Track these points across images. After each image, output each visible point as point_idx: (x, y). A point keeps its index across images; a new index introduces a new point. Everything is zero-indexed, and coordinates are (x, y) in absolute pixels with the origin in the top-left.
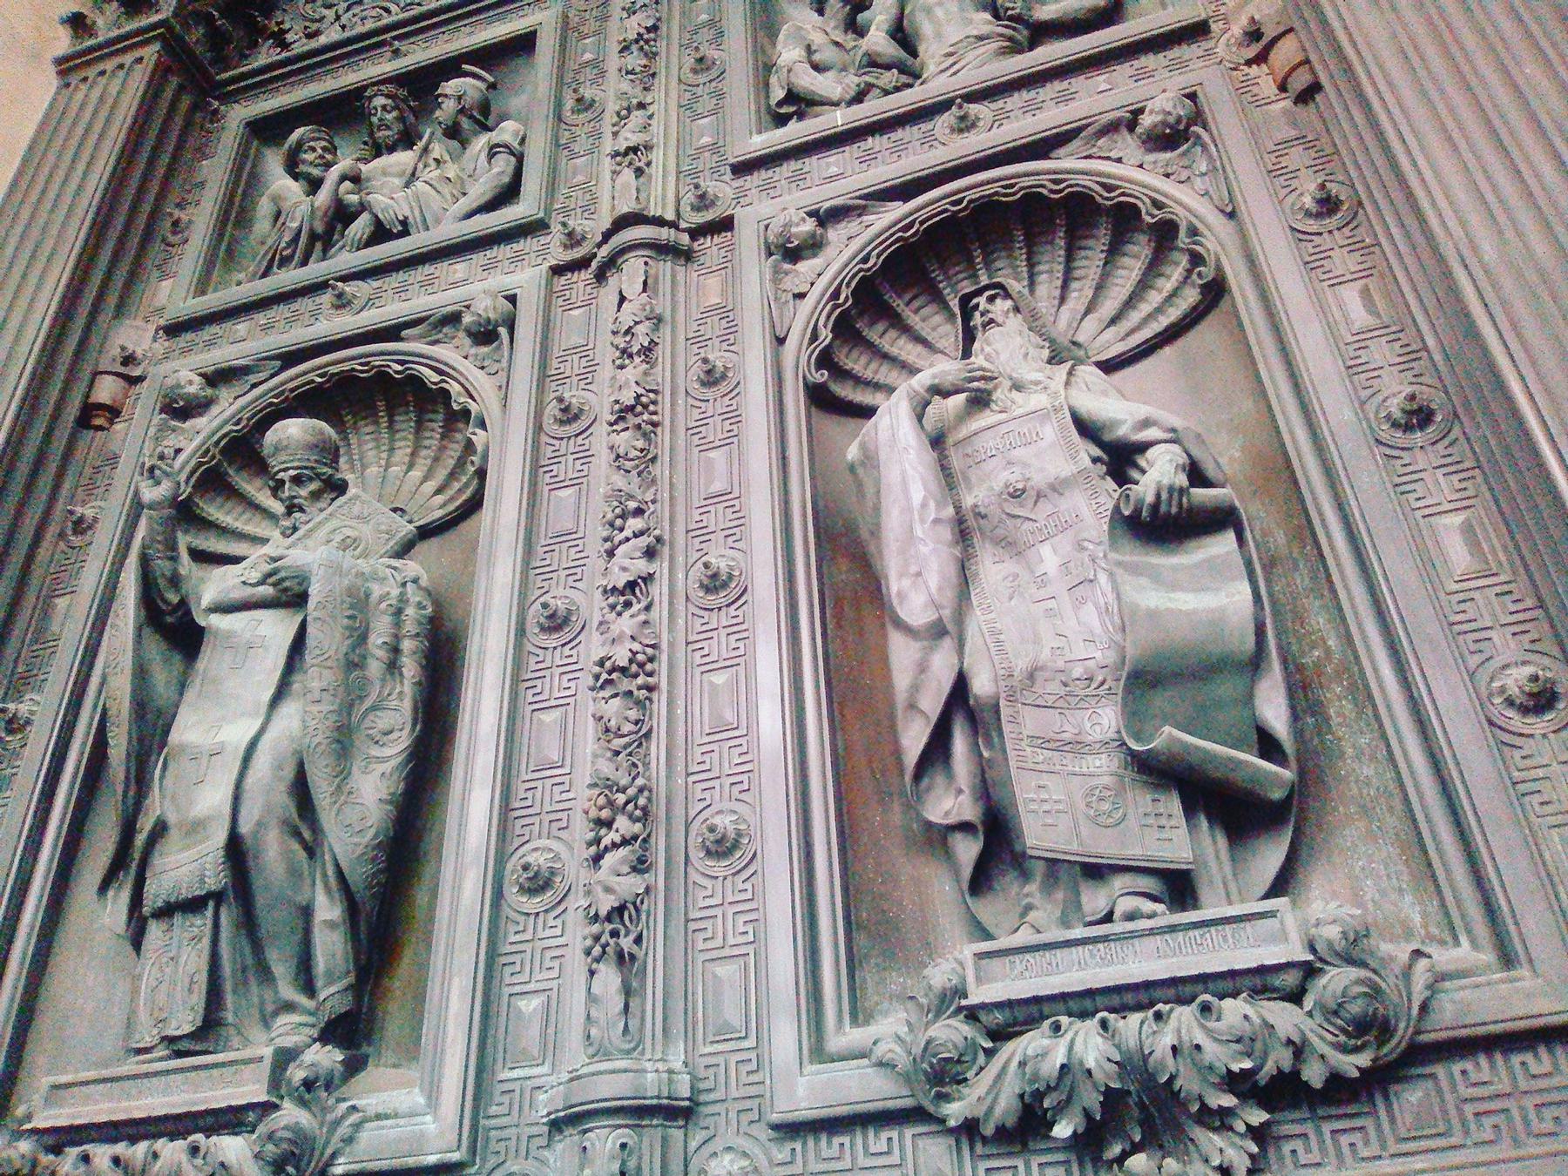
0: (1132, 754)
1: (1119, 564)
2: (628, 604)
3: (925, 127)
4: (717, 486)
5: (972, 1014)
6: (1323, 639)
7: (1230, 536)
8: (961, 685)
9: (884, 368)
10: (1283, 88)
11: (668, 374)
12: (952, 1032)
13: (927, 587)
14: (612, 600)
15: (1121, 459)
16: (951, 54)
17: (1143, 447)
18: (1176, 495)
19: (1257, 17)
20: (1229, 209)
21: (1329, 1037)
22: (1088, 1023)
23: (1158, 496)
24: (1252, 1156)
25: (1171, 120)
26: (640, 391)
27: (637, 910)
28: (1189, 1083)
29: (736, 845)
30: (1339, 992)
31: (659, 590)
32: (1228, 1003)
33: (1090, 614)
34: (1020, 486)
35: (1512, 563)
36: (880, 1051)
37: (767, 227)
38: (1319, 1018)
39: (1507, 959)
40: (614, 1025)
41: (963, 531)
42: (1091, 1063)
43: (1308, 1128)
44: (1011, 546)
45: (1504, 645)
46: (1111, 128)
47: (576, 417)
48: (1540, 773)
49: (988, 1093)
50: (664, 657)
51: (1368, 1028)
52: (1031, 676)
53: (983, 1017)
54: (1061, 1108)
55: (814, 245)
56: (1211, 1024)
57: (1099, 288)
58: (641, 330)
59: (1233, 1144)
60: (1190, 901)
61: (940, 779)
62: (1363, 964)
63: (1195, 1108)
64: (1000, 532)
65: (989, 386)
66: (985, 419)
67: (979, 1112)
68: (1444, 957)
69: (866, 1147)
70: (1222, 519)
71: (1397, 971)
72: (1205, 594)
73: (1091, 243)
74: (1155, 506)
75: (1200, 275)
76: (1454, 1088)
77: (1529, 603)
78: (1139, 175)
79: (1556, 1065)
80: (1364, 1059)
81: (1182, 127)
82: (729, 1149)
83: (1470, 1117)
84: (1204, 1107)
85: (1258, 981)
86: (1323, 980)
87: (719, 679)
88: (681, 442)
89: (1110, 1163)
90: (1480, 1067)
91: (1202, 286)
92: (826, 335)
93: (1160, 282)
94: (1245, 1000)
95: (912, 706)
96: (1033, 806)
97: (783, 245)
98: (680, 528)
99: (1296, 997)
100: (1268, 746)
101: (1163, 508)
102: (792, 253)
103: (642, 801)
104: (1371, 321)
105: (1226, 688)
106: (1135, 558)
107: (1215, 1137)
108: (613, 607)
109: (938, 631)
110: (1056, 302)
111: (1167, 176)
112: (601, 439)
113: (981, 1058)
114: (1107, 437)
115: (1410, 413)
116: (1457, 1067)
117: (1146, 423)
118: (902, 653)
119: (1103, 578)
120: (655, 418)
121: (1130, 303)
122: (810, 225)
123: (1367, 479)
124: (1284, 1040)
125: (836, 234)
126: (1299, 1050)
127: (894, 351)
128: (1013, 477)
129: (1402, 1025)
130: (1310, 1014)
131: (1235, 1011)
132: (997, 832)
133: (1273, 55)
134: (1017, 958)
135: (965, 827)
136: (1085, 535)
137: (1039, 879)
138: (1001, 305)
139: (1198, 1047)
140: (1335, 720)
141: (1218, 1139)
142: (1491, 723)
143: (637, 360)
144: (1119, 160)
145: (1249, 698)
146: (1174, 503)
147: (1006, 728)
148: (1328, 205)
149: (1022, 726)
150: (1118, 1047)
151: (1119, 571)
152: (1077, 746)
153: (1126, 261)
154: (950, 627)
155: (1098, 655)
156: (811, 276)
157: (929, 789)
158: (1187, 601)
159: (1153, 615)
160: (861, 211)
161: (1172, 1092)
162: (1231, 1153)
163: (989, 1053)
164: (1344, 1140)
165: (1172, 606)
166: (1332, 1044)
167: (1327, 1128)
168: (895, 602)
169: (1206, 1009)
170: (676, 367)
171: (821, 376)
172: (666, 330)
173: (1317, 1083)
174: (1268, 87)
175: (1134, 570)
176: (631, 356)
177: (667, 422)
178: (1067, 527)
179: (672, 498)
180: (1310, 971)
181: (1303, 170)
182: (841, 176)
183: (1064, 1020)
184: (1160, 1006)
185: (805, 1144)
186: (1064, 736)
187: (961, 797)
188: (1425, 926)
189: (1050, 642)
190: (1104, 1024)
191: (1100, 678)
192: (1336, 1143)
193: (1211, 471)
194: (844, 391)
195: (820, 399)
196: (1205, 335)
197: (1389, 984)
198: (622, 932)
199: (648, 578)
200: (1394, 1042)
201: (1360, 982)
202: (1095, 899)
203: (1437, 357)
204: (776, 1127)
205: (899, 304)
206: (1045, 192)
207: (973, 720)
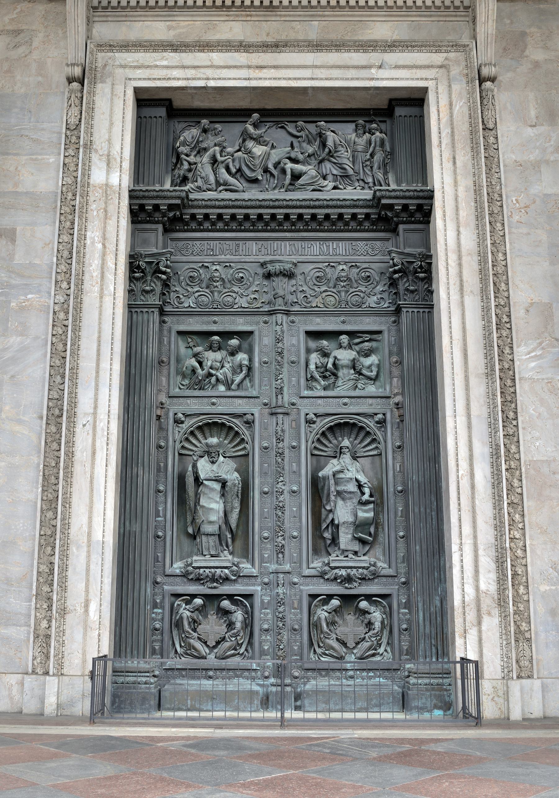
8: (333, 520)
12: (327, 568)
28: (354, 578)
31: (285, 492)
37: (307, 414)
39: (390, 567)
51: (374, 574)
55: (314, 422)
90: (384, 578)
95: (324, 520)
109: (331, 511)
117: (365, 483)
118: (324, 512)
123: (392, 501)
125: (318, 420)
131: (360, 570)
132: (335, 541)
148: (399, 447)
175: (360, 509)
202: (346, 554)
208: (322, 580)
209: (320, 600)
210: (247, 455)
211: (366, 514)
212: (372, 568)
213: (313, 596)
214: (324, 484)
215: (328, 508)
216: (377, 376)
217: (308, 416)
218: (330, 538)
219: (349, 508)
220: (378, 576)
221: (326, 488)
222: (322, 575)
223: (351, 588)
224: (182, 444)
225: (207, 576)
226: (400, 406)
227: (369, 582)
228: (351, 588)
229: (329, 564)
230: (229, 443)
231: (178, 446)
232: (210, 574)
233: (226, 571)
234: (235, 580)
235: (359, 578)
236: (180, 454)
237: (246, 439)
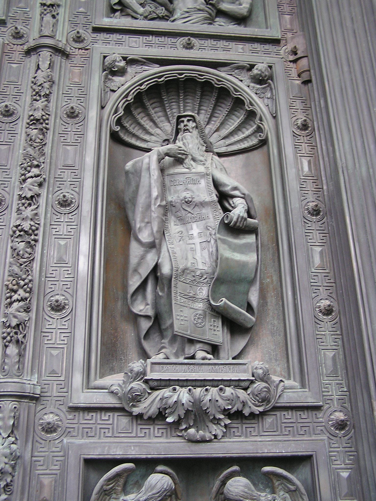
0: (210, 304)
1: (219, 239)
2: (30, 205)
3: (173, 40)
4: (70, 162)
5: (146, 382)
6: (271, 276)
7: (254, 237)
8: (156, 268)
9: (140, 131)
10: (299, 76)
11: (54, 107)
13: (152, 229)
14: (23, 201)
15: (224, 198)
16: (188, 12)
17: (233, 197)
18: (243, 220)
19: (297, 47)
20: (274, 115)
21: (253, 402)
22: (184, 389)
23: (238, 219)
24: (223, 432)
25: (263, 75)
26: (44, 113)
27: (25, 326)
28: (212, 411)
29: (64, 308)
30: (260, 388)
31: (42, 201)
32: (227, 389)
33: (206, 253)
34: (190, 199)
35: (330, 266)
36: (113, 388)
37: (105, 57)
38: (251, 396)
39: (303, 386)
40: (14, 366)
41: (167, 209)
42: (184, 402)
43: (239, 425)
44: (182, 221)
45: (323, 292)
46: (240, 68)
47: (11, 115)
48: (323, 333)
49: (148, 406)
50: (41, 229)
51: (266, 400)
52: (183, 271)
53: (151, 383)
54: (171, 414)
55: (122, 72)
56: (221, 394)
57: (222, 124)
58: (46, 85)
59: (219, 429)
60: (216, 354)
61: (140, 298)
62: (266, 382)
63: (212, 417)
64: (179, 214)
65: (184, 157)
66: (180, 169)
67: (144, 412)
68: (287, 383)
69: (101, 417)
70: (253, 230)
71: (275, 384)
72: (243, 254)
73: (223, 105)
74: (236, 222)
75: (260, 135)
76: (281, 419)
77: (332, 281)
78: (246, 89)
79: (308, 416)
80: (261, 409)
81: (266, 79)
82: (52, 413)
83: (283, 427)
84: (214, 418)
85: (237, 383)
86: (255, 385)
87: (62, 242)
88: (56, 139)
89: (182, 430)
90: (289, 414)
91: (259, 140)
92: (121, 112)
93: (244, 130)
94: (232, 389)
95: (136, 270)
96: (178, 318)
97: (111, 68)
98: (52, 176)
99: (246, 389)
100: (249, 308)
101: (238, 224)
102: (112, 71)
103: (30, 285)
104: (309, 174)
105: (242, 288)
106: (224, 238)
107: (214, 426)
108: (23, 204)
109: (152, 246)
110: (206, 123)
111: (256, 94)
112: (21, 127)
113: (147, 395)
114: (221, 189)
115: (315, 210)
116: (283, 413)
117: (235, 189)
118: (135, 250)
119: (213, 242)
120: (47, 126)
121: (231, 134)
122: (122, 64)
123: (298, 229)
124: (242, 402)
125: (131, 70)
126: (244, 404)
127: (142, 122)
128: (187, 195)
129: (273, 401)
130: (249, 394)
131: (229, 391)
133: (299, 62)
134: (165, 366)
135: (147, 317)
136: (209, 224)
137: (168, 339)
138: (191, 124)
139: (217, 401)
140: (269, 304)
141: (215, 427)
142: (315, 316)
143: (43, 99)
144: (241, 81)
145: (247, 293)
146: (242, 223)
147: (173, 288)
148: (305, 127)
149: (178, 288)
150: (193, 397)
151: (219, 241)
152: (193, 298)
153: (234, 117)
154: (158, 246)
155: (206, 268)
156: (118, 84)
157: (135, 300)
158: (238, 257)
159: (227, 259)
160: (143, 64)
161: (206, 412)
162: (218, 430)
163: (149, 394)
164: (249, 430)
165: (233, 257)
166: (253, 404)
167: (244, 426)
168: (137, 231)
169: (221, 389)
170: (58, 105)
171: (118, 128)
172: (55, 88)
173: (247, 414)
174: (294, 73)
175: (224, 242)
176: (40, 96)
177: (52, 129)
178: (203, 219)
179: (51, 163)
180: (252, 382)
181: (299, 110)
182: (137, 47)
183: (177, 387)
184: (207, 387)
185: (79, 414)
186: (191, 294)
187: (148, 307)
188: (281, 371)
189: (191, 260)
190: (190, 390)
191: (205, 277)
192: (246, 430)
193: (252, 213)
194: (122, 135)
195: (115, 137)
196: (256, 155)
197: (272, 388)
198: (19, 333)
199: (39, 195)
200: (270, 405)
201: (265, 387)
202: (189, 350)
203: (325, 193)
204: (70, 408)
205: (148, 104)
206: (213, 82)
207: (157, 279)
208: (124, 421)
209: (118, 475)
211: (243, 254)
212: (259, 385)
213: (96, 465)
214: (138, 187)
215: (145, 236)
216: (250, 11)
218: (150, 312)
219: (197, 240)
220: (275, 408)
221: (142, 191)
222: (124, 408)
223: (203, 441)
226: (300, 54)
227: (252, 427)
228: (203, 441)
229: (144, 373)
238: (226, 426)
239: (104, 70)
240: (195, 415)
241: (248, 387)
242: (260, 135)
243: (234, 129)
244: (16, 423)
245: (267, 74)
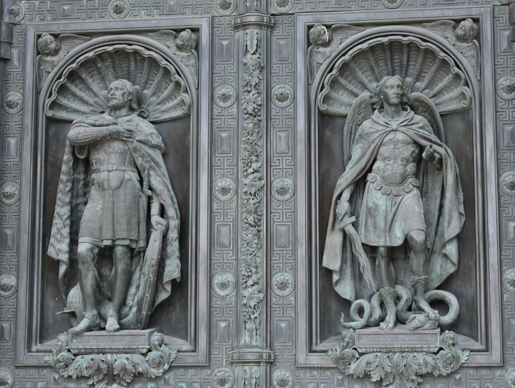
25: (468, 35)
37: (310, 27)
53: (358, 349)
111: (462, 53)
160: (348, 28)
163: (358, 359)
183: (379, 354)
206: (418, 44)
210: (187, 117)
217: (312, 30)
224: (53, 98)
225: (99, 370)
230: (154, 94)
231: (45, 101)
232: (104, 366)
233: (137, 358)
234: (157, 379)
235: (416, 375)
236: (51, 121)
237: (183, 83)
238: (419, 384)
239: (309, 44)
240: (394, 376)
241: (438, 352)
242: (464, 103)
243: (442, 87)
244: (258, 381)
245: (471, 33)
